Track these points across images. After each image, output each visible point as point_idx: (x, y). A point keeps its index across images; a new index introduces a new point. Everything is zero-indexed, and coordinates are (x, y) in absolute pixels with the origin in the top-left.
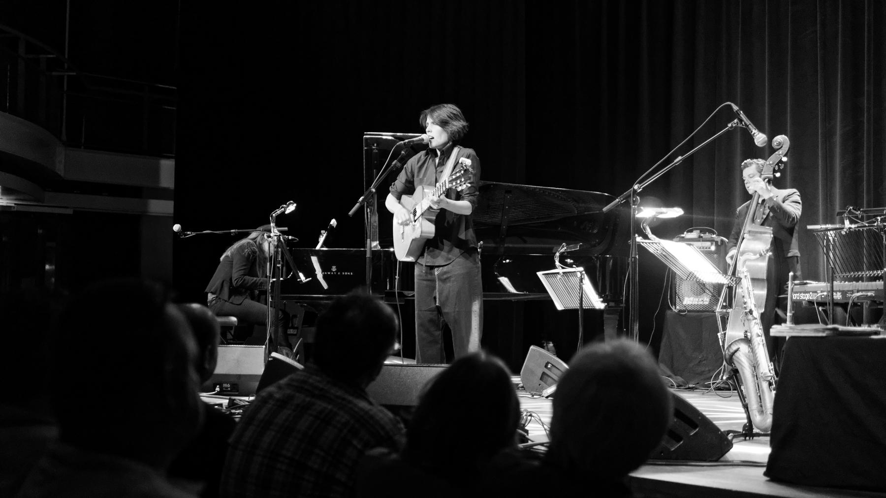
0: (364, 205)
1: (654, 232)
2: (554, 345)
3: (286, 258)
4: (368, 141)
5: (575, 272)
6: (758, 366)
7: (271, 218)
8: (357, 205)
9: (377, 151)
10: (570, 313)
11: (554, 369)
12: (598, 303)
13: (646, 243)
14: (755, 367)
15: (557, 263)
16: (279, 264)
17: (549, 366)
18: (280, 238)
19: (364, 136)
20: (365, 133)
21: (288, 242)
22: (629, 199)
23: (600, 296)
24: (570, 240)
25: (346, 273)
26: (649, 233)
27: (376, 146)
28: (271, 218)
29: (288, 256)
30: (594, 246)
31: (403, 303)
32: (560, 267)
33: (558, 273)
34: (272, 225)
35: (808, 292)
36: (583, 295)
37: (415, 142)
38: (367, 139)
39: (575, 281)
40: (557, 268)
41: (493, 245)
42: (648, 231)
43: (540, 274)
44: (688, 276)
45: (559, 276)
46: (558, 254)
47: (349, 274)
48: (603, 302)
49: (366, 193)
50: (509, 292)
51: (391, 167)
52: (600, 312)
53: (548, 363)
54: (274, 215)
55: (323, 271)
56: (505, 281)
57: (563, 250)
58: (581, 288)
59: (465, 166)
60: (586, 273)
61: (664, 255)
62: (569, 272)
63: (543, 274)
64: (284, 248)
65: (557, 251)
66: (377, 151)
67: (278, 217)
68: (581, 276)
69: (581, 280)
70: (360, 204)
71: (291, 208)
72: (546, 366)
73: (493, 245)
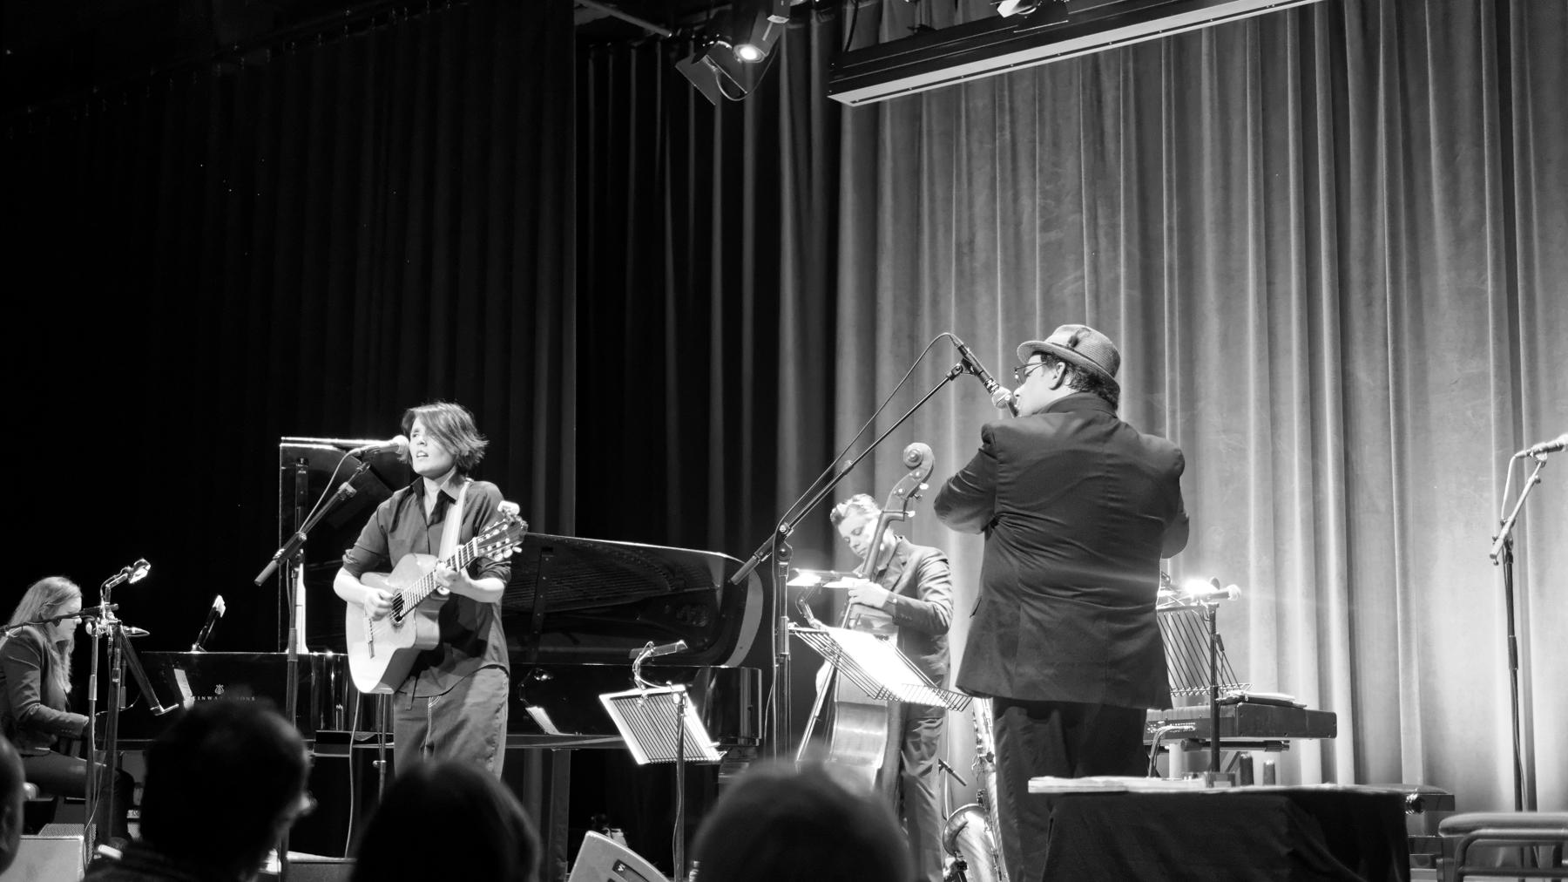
4: (289, 453)
7: (101, 592)
9: (305, 472)
10: (661, 771)
12: (708, 750)
15: (638, 678)
16: (116, 677)
18: (119, 630)
19: (282, 445)
20: (283, 438)
21: (135, 640)
23: (714, 739)
27: (304, 463)
28: (101, 592)
32: (643, 686)
33: (639, 696)
34: (103, 604)
36: (685, 737)
40: (637, 687)
43: (605, 699)
44: (495, 539)
45: (640, 701)
46: (638, 662)
47: (248, 699)
48: (719, 749)
50: (547, 734)
52: (714, 768)
54: (107, 586)
59: (512, 516)
60: (689, 695)
63: (612, 699)
64: (126, 649)
66: (305, 472)
67: (115, 589)
68: (681, 702)
69: (681, 708)
71: (141, 573)
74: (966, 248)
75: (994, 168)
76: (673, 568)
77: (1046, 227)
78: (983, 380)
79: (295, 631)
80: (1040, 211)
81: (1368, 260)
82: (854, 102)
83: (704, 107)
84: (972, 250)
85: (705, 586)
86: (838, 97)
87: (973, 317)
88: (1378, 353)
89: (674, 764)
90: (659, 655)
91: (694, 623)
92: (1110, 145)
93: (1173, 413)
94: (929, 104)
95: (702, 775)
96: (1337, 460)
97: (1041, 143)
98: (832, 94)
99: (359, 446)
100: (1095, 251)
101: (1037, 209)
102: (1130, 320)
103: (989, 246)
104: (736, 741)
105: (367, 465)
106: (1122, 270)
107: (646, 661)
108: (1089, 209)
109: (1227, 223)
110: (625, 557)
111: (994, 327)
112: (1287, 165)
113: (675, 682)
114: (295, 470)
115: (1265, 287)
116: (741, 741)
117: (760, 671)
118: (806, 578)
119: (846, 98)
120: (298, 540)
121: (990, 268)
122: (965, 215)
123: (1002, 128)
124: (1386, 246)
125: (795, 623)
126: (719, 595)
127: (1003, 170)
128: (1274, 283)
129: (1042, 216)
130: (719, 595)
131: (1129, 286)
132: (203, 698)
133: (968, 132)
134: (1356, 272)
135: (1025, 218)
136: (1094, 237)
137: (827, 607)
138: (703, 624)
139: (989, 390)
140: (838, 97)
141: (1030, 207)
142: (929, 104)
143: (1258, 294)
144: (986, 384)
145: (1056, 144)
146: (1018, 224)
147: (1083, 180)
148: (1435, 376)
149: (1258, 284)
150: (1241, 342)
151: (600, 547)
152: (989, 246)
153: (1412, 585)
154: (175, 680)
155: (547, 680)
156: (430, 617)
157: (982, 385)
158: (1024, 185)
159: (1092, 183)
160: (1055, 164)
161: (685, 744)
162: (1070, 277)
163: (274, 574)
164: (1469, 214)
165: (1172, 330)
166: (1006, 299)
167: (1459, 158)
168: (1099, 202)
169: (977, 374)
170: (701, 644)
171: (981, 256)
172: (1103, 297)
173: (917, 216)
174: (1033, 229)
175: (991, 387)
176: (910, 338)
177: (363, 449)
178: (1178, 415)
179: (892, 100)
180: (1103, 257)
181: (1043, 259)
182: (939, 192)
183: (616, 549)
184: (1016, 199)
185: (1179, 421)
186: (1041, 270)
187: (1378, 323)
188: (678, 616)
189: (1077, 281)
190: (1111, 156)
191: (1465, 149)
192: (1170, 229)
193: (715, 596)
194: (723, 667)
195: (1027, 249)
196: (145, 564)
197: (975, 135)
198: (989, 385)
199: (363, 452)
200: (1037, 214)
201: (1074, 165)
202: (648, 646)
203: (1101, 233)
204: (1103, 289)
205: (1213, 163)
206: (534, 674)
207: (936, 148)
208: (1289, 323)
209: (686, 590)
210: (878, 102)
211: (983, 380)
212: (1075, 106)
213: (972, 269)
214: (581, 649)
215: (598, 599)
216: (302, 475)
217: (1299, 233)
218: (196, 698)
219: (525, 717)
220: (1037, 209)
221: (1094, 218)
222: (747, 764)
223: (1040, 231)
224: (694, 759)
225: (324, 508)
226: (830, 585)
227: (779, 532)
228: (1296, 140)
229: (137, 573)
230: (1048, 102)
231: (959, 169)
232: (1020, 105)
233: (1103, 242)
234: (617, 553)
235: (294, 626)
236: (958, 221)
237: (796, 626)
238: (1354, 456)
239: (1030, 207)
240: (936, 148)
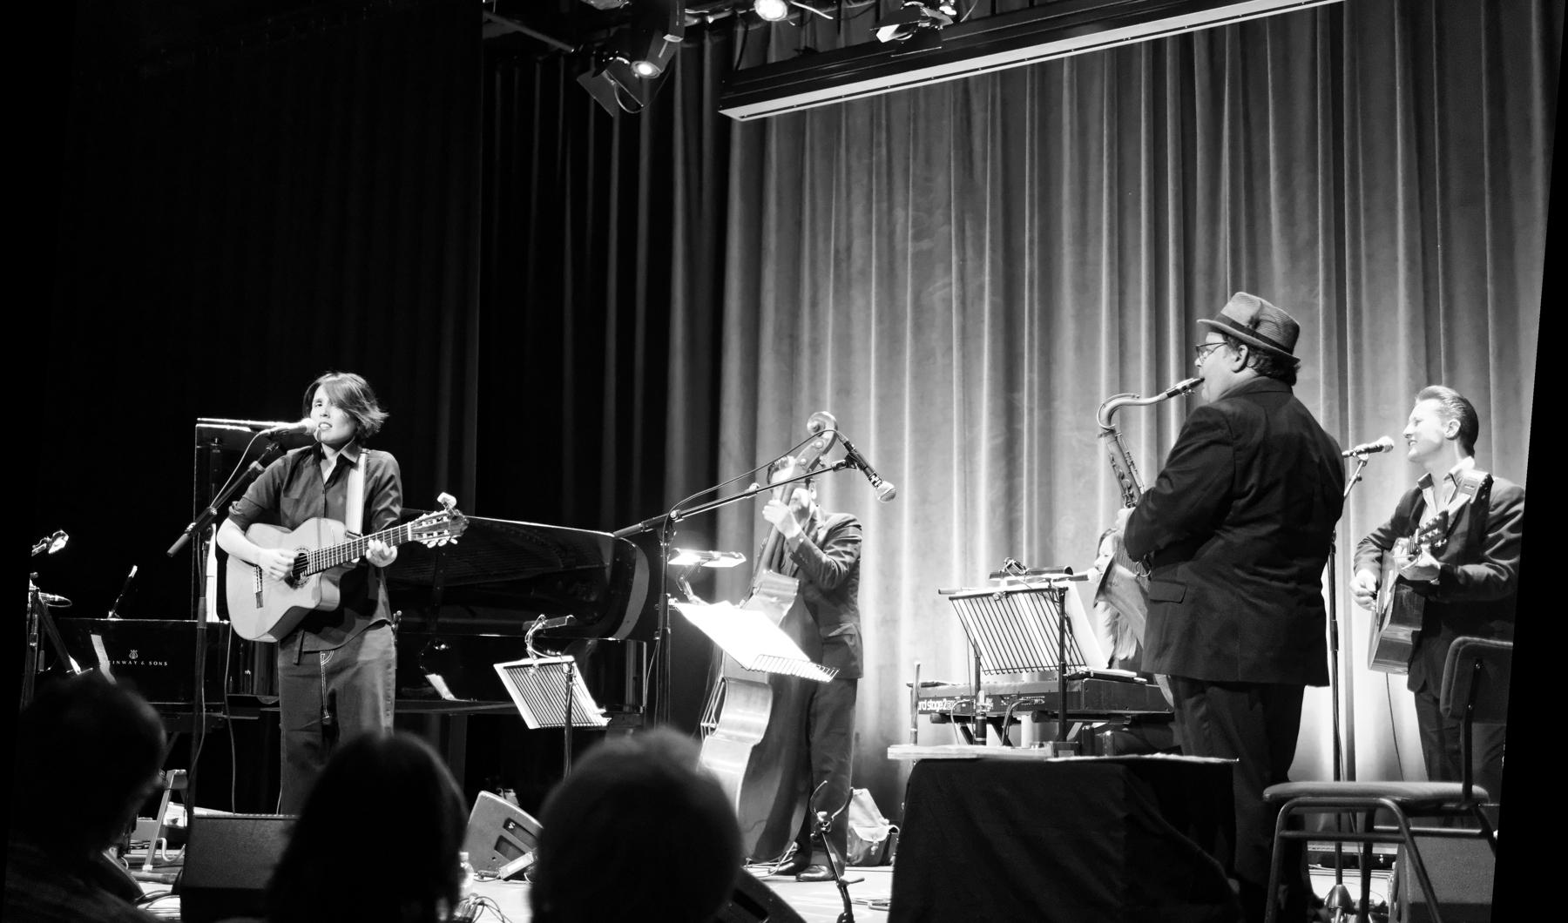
1: (695, 593)
5: (559, 663)
9: (219, 451)
10: (550, 735)
11: (519, 830)
15: (530, 649)
17: (511, 826)
19: (197, 425)
20: (199, 419)
23: (600, 706)
31: (256, 718)
32: (534, 656)
33: (531, 666)
35: (940, 699)
36: (573, 704)
38: (200, 429)
40: (529, 657)
43: (499, 668)
45: (532, 671)
46: (530, 633)
47: (161, 664)
48: (604, 715)
50: (444, 699)
53: (508, 821)
57: (539, 626)
58: (570, 691)
62: (549, 664)
63: (505, 668)
65: (529, 627)
66: (219, 451)
68: (570, 671)
69: (570, 678)
72: (506, 826)
74: (843, 257)
76: (565, 545)
77: (917, 237)
79: (205, 600)
80: (913, 222)
82: (743, 117)
83: (603, 118)
84: (849, 257)
85: (595, 564)
87: (848, 318)
90: (550, 627)
91: (585, 598)
93: (1031, 410)
95: (588, 736)
97: (915, 159)
98: (723, 109)
99: (269, 427)
100: (963, 260)
102: (993, 325)
103: (865, 253)
104: (621, 709)
105: (276, 446)
106: (987, 279)
107: (537, 633)
109: (1083, 237)
110: (521, 535)
112: (1139, 185)
114: (209, 449)
115: (1116, 298)
116: (626, 709)
117: (645, 644)
118: (686, 557)
119: (736, 113)
120: (210, 515)
121: (865, 273)
122: (843, 227)
123: (879, 145)
124: (1228, 254)
125: (676, 599)
126: (608, 572)
129: (914, 226)
130: (608, 572)
131: (993, 294)
132: (118, 662)
134: (1200, 285)
135: (899, 228)
138: (593, 599)
141: (903, 218)
143: (1111, 303)
145: (928, 161)
146: (891, 234)
147: (953, 194)
149: (1111, 294)
150: (1094, 346)
151: (498, 527)
155: (445, 650)
156: (334, 583)
158: (899, 197)
160: (928, 180)
161: (573, 710)
162: (939, 284)
163: (188, 545)
164: (1303, 234)
165: (1031, 334)
166: (879, 304)
170: (591, 618)
171: (857, 263)
172: (969, 302)
173: (799, 224)
174: (905, 239)
177: (273, 430)
178: (1036, 413)
179: (777, 116)
180: (970, 264)
183: (513, 528)
184: (891, 209)
185: (1036, 419)
186: (912, 277)
193: (604, 572)
194: (610, 639)
197: (854, 150)
199: (272, 433)
201: (946, 179)
202: (540, 619)
204: (970, 295)
209: (579, 567)
210: (765, 118)
212: (948, 126)
214: (476, 621)
216: (217, 454)
217: (1149, 249)
218: (111, 663)
221: (961, 230)
222: (631, 731)
223: (912, 241)
224: (585, 725)
225: (236, 483)
226: (709, 564)
230: (922, 124)
231: (838, 185)
233: (970, 253)
235: (205, 595)
236: (837, 229)
237: (676, 602)
239: (903, 218)
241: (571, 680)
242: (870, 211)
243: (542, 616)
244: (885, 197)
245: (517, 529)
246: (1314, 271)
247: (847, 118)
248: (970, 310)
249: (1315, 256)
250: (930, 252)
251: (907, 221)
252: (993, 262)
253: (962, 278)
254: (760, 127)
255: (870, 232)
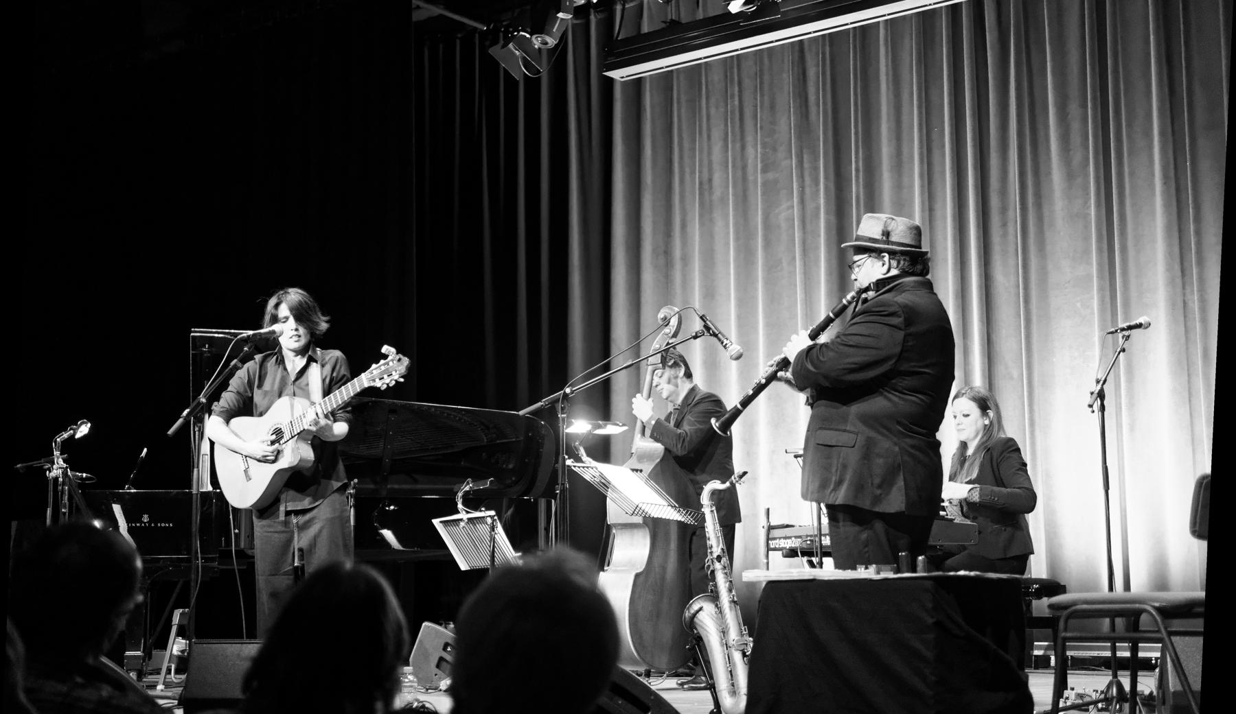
0: (190, 421)
1: (588, 455)
2: (455, 627)
3: (76, 503)
5: (484, 517)
6: (728, 632)
8: (180, 421)
9: (209, 355)
10: (477, 574)
13: (579, 467)
14: (724, 632)
15: (460, 506)
20: (193, 329)
22: (556, 405)
24: (477, 477)
25: (163, 525)
26: (582, 455)
27: (208, 348)
29: (78, 499)
30: (510, 486)
31: (245, 567)
32: (464, 512)
33: (461, 520)
37: (263, 336)
39: (483, 529)
41: (372, 486)
42: (582, 452)
43: (436, 522)
46: (460, 494)
49: (193, 405)
50: (394, 549)
51: (229, 368)
55: (128, 520)
56: (388, 534)
57: (467, 488)
58: (493, 539)
61: (602, 483)
63: (441, 522)
69: (493, 528)
70: (185, 419)
71: (84, 430)
73: (372, 486)
74: (706, 186)
75: (726, 125)
77: (765, 170)
78: (719, 340)
81: (1004, 192)
82: (623, 77)
83: (511, 82)
84: (711, 187)
86: (610, 74)
87: (712, 236)
88: (1012, 262)
89: (488, 569)
91: (504, 466)
92: (813, 109)
94: (678, 78)
96: (982, 339)
97: (761, 107)
101: (759, 155)
103: (723, 183)
106: (822, 201)
107: (467, 493)
108: (797, 156)
111: (728, 244)
112: (943, 122)
113: (488, 509)
119: (616, 74)
121: (724, 200)
122: (706, 162)
123: (732, 96)
127: (733, 127)
128: (934, 210)
129: (762, 162)
131: (827, 213)
132: (133, 525)
133: (708, 98)
134: (994, 201)
135: (750, 162)
136: (801, 177)
137: (602, 450)
138: (511, 466)
139: (725, 347)
140: (610, 74)
141: (754, 154)
142: (678, 78)
144: (722, 343)
145: (772, 107)
146: (744, 168)
147: (792, 134)
148: (1053, 277)
149: (923, 211)
152: (723, 183)
153: (1038, 433)
154: (113, 512)
157: (719, 344)
158: (749, 138)
159: (799, 138)
160: (773, 123)
162: (784, 206)
164: (1077, 157)
166: (736, 224)
167: (1069, 116)
168: (804, 151)
169: (715, 335)
170: (510, 481)
171: (717, 193)
175: (726, 344)
176: (665, 252)
179: (650, 75)
180: (808, 190)
181: (763, 194)
182: (686, 145)
184: (743, 148)
187: (1011, 238)
188: (493, 461)
189: (789, 210)
190: (813, 116)
191: (1074, 109)
192: (857, 170)
195: (751, 186)
196: (86, 423)
197: (713, 101)
198: (724, 344)
200: (759, 160)
201: (786, 123)
203: (807, 174)
205: (888, 120)
206: (385, 506)
207: (683, 111)
208: (946, 239)
209: (498, 441)
211: (719, 340)
212: (787, 80)
213: (711, 201)
214: (419, 486)
215: (432, 449)
217: (952, 172)
218: (128, 525)
219: (378, 538)
220: (759, 155)
223: (761, 173)
227: (565, 392)
228: (950, 103)
229: (80, 430)
230: (766, 77)
231: (700, 126)
232: (747, 83)
234: (445, 414)
236: (700, 165)
238: (994, 337)
239: (754, 154)
240: (684, 104)
241: (494, 531)
242: (727, 151)
243: (469, 479)
244: (738, 137)
245: (449, 412)
246: (1086, 189)
247: (706, 78)
248: (809, 227)
249: (1087, 175)
250: (776, 182)
251: (756, 157)
252: (826, 188)
253: (802, 201)
254: (638, 83)
255: (727, 166)
